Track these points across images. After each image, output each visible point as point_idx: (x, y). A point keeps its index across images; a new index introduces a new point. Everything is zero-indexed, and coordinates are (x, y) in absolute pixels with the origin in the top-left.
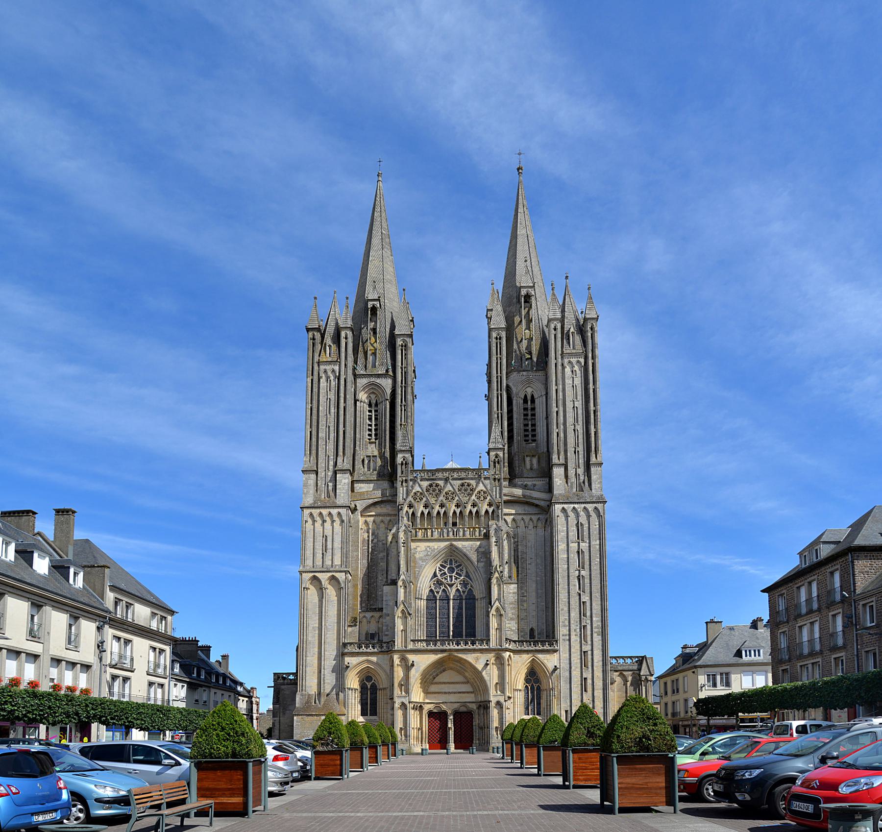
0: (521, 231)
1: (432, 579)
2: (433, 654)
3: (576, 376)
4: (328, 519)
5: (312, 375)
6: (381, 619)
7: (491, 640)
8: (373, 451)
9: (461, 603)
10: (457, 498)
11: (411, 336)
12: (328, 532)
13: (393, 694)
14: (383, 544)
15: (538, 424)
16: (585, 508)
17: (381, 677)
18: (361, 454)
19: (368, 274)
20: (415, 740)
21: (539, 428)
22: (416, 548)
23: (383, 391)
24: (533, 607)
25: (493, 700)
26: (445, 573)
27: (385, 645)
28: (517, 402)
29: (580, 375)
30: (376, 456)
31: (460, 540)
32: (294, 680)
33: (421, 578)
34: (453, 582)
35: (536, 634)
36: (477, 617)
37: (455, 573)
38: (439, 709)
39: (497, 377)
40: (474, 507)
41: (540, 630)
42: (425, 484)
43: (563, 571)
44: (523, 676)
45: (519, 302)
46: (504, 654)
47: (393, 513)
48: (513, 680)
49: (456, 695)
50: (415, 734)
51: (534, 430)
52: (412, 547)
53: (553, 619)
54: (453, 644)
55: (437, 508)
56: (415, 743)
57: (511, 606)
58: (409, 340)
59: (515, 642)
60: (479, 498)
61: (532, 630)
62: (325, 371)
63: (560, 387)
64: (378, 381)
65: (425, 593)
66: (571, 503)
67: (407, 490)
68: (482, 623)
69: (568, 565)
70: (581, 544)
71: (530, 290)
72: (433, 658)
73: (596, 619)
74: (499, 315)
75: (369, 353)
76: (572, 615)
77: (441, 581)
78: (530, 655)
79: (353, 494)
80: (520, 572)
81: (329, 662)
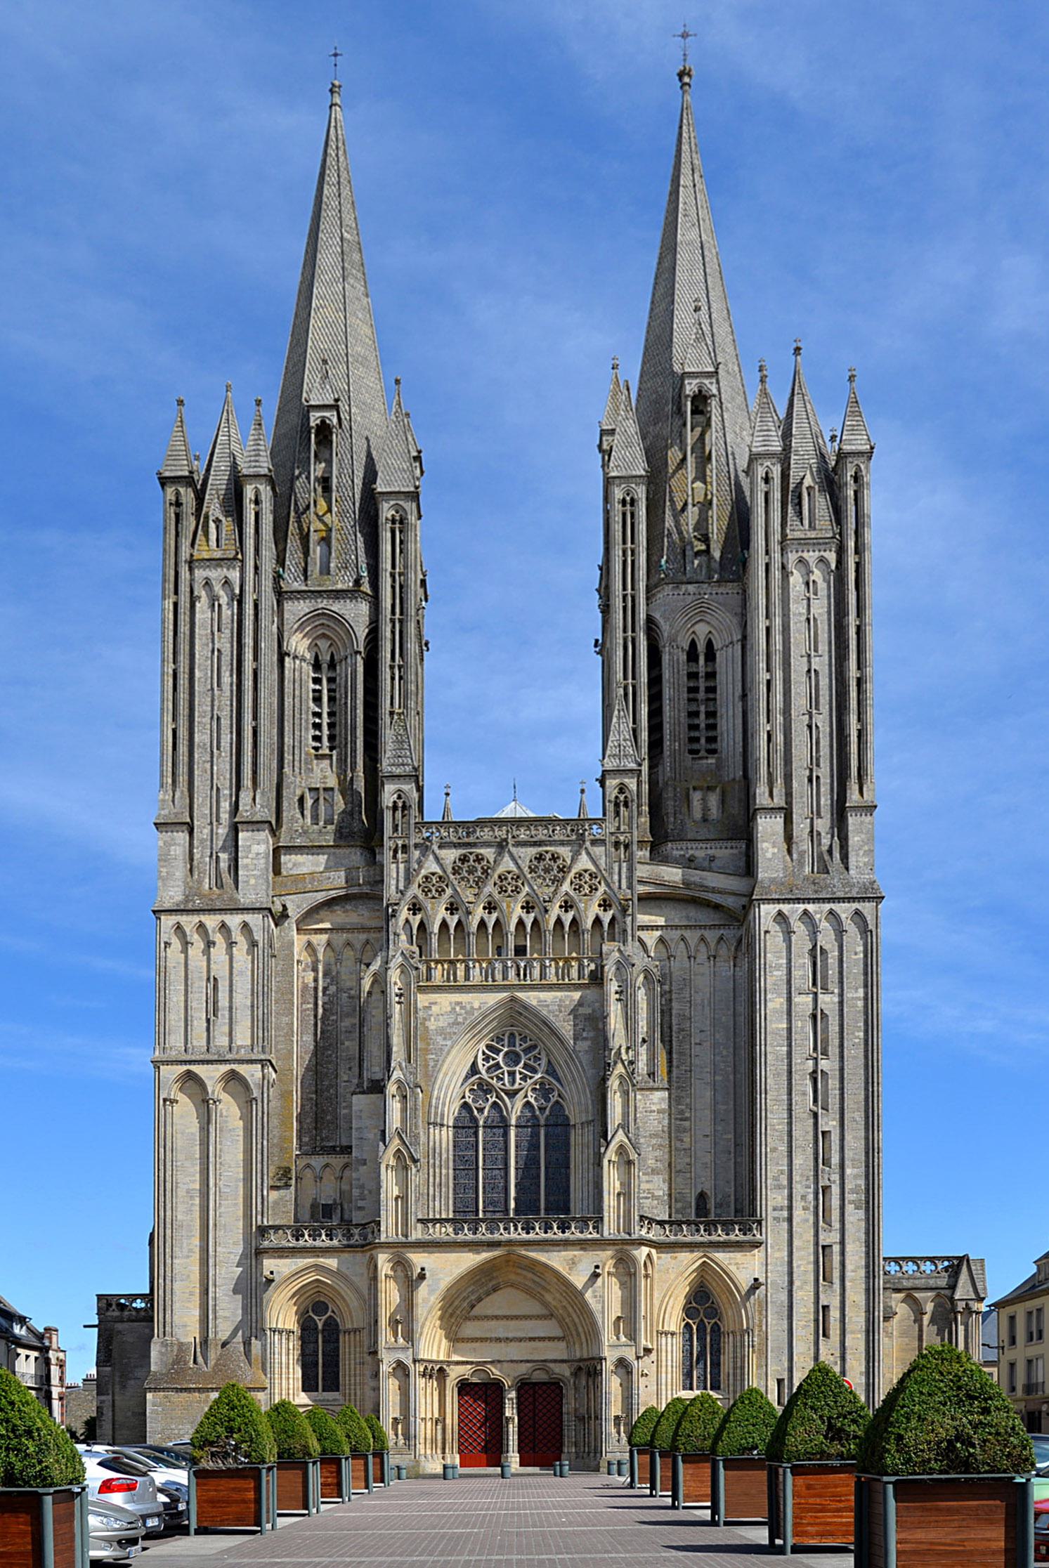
0: (686, 235)
1: (467, 1078)
2: (470, 1251)
3: (816, 594)
4: (218, 938)
5: (176, 592)
6: (347, 1173)
7: (606, 1219)
8: (325, 777)
9: (535, 1135)
10: (527, 889)
11: (414, 496)
12: (219, 968)
13: (376, 1342)
15: (721, 711)
16: (831, 912)
17: (348, 1306)
18: (296, 785)
19: (310, 343)
20: (428, 1446)
21: (724, 721)
23: (349, 632)
24: (707, 1144)
25: (610, 1356)
26: (497, 1066)
27: (356, 1231)
28: (674, 659)
29: (825, 592)
30: (332, 789)
31: (533, 987)
32: (145, 1309)
33: (441, 1076)
34: (516, 1086)
35: (711, 1205)
37: (521, 1064)
38: (483, 1375)
39: (625, 597)
40: (566, 911)
41: (720, 1196)
42: (450, 855)
43: (777, 1060)
44: (680, 1301)
45: (680, 412)
46: (635, 1253)
47: (374, 923)
48: (655, 1316)
49: (522, 1344)
50: (429, 1432)
52: (420, 1005)
53: (752, 1171)
54: (516, 1229)
55: (479, 912)
56: (429, 1452)
57: (654, 1141)
58: (409, 506)
59: (661, 1223)
60: (578, 889)
61: (702, 1197)
62: (208, 584)
63: (778, 621)
64: (336, 606)
65: (451, 1112)
66: (798, 900)
67: (407, 870)
68: (585, 1181)
69: (790, 1045)
70: (820, 996)
71: (706, 382)
72: (470, 1260)
73: (854, 1173)
74: (629, 445)
75: (314, 537)
76: (797, 1161)
77: (488, 1084)
78: (697, 1254)
79: (279, 879)
80: (675, 1063)
81: (227, 1270)
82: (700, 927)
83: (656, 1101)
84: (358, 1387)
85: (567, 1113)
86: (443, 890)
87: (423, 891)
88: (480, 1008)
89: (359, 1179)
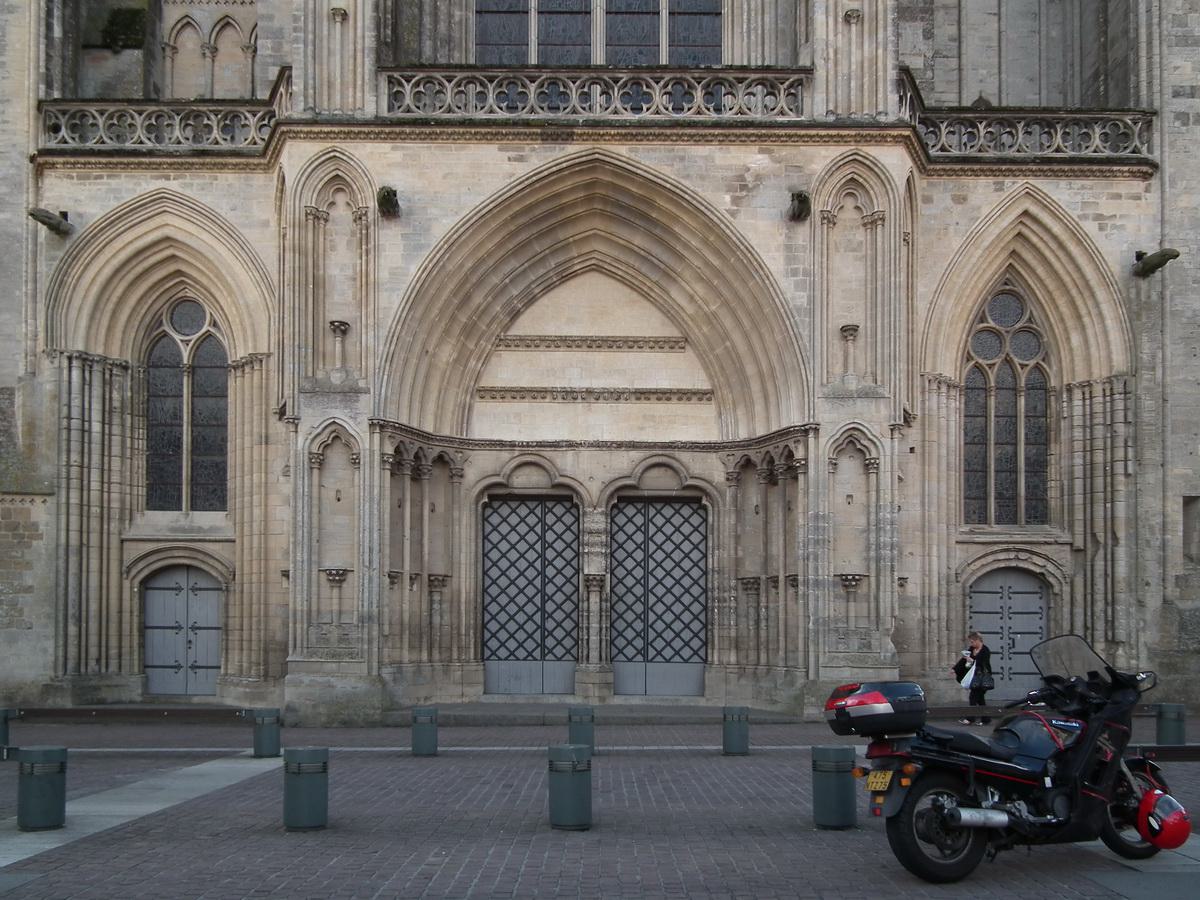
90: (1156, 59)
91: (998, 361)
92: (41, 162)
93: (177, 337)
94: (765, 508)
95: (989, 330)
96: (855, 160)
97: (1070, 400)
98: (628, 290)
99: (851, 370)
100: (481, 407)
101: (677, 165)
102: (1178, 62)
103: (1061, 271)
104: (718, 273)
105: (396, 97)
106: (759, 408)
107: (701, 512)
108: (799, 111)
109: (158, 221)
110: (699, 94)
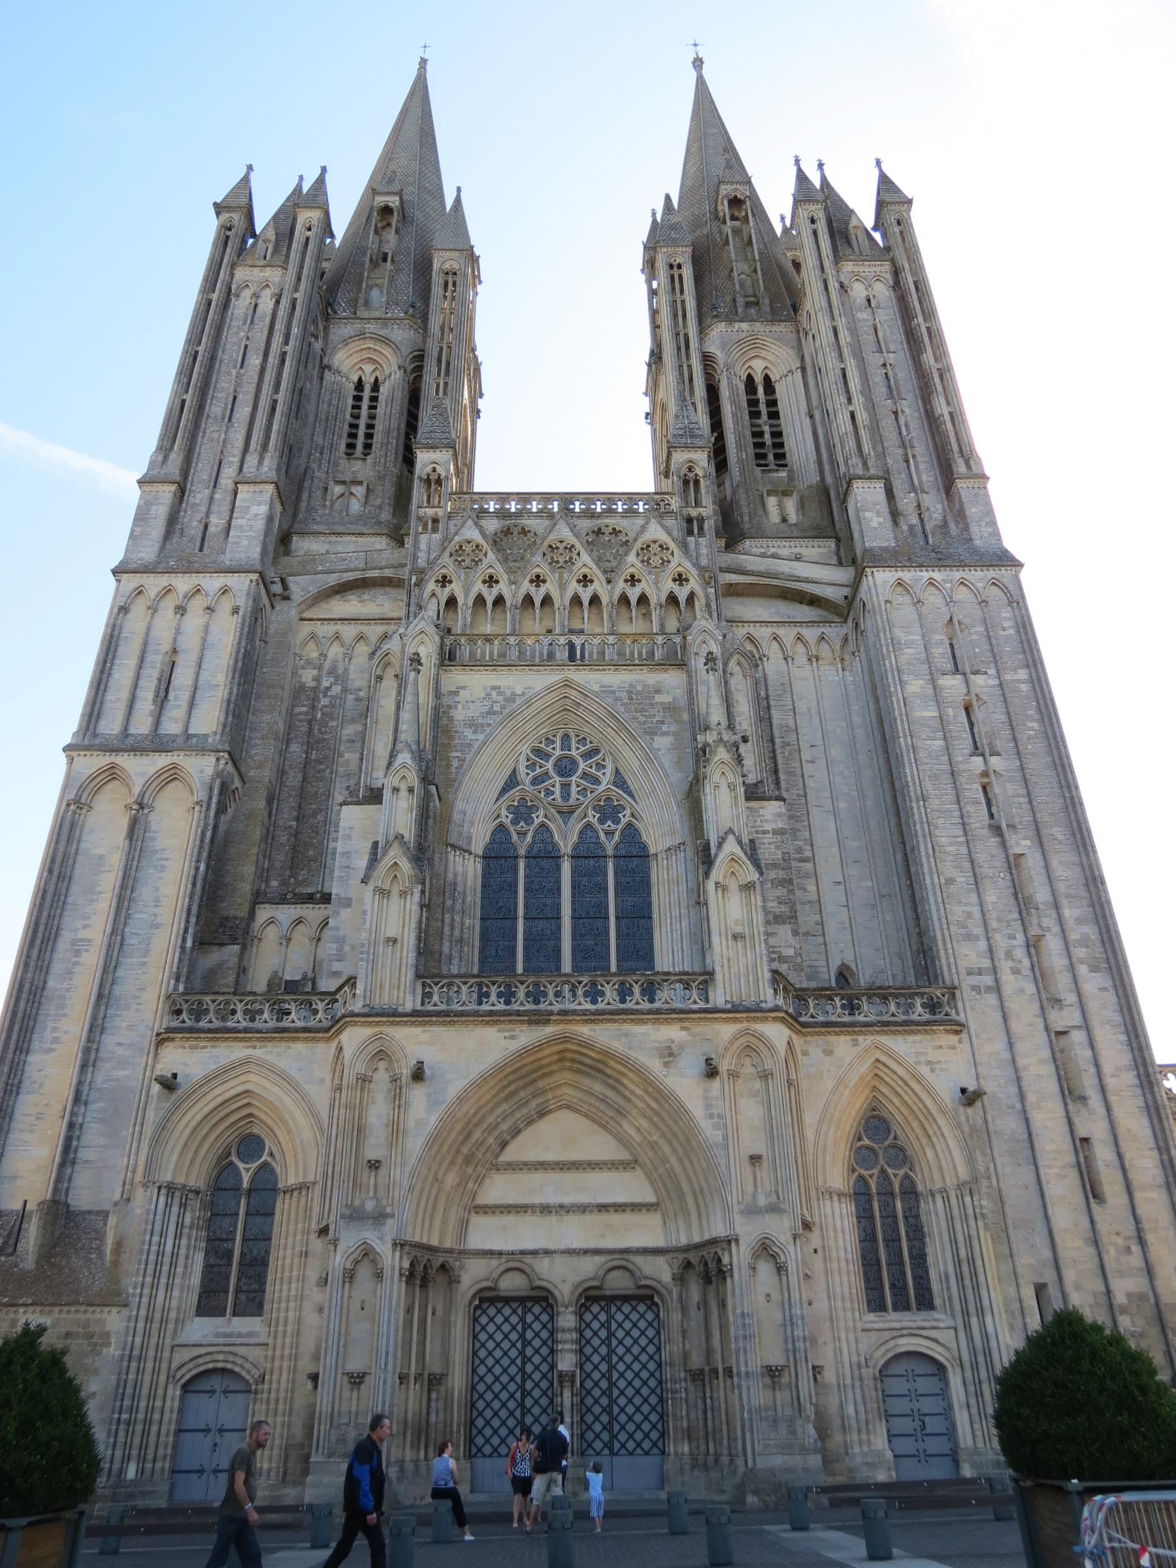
1: (504, 791)
14: (359, 700)
22: (456, 693)
27: (320, 1006)
34: (572, 801)
36: (655, 916)
40: (633, 585)
51: (781, 445)
65: (480, 837)
82: (796, 623)
83: (769, 817)
84: (292, 1304)
85: (644, 838)
86: (480, 560)
87: (456, 560)
88: (524, 694)
89: (338, 929)
90: (950, 951)
91: (875, 1171)
92: (162, 1039)
93: (241, 1166)
94: (704, 1304)
95: (867, 1148)
96: (747, 1033)
97: (934, 1202)
98: (591, 1123)
99: (759, 1189)
100: (477, 1221)
101: (623, 1040)
102: (966, 952)
103: (910, 1102)
104: (657, 1113)
105: (427, 996)
106: (694, 1218)
107: (654, 1308)
108: (707, 1001)
109: (243, 1078)
110: (637, 990)
